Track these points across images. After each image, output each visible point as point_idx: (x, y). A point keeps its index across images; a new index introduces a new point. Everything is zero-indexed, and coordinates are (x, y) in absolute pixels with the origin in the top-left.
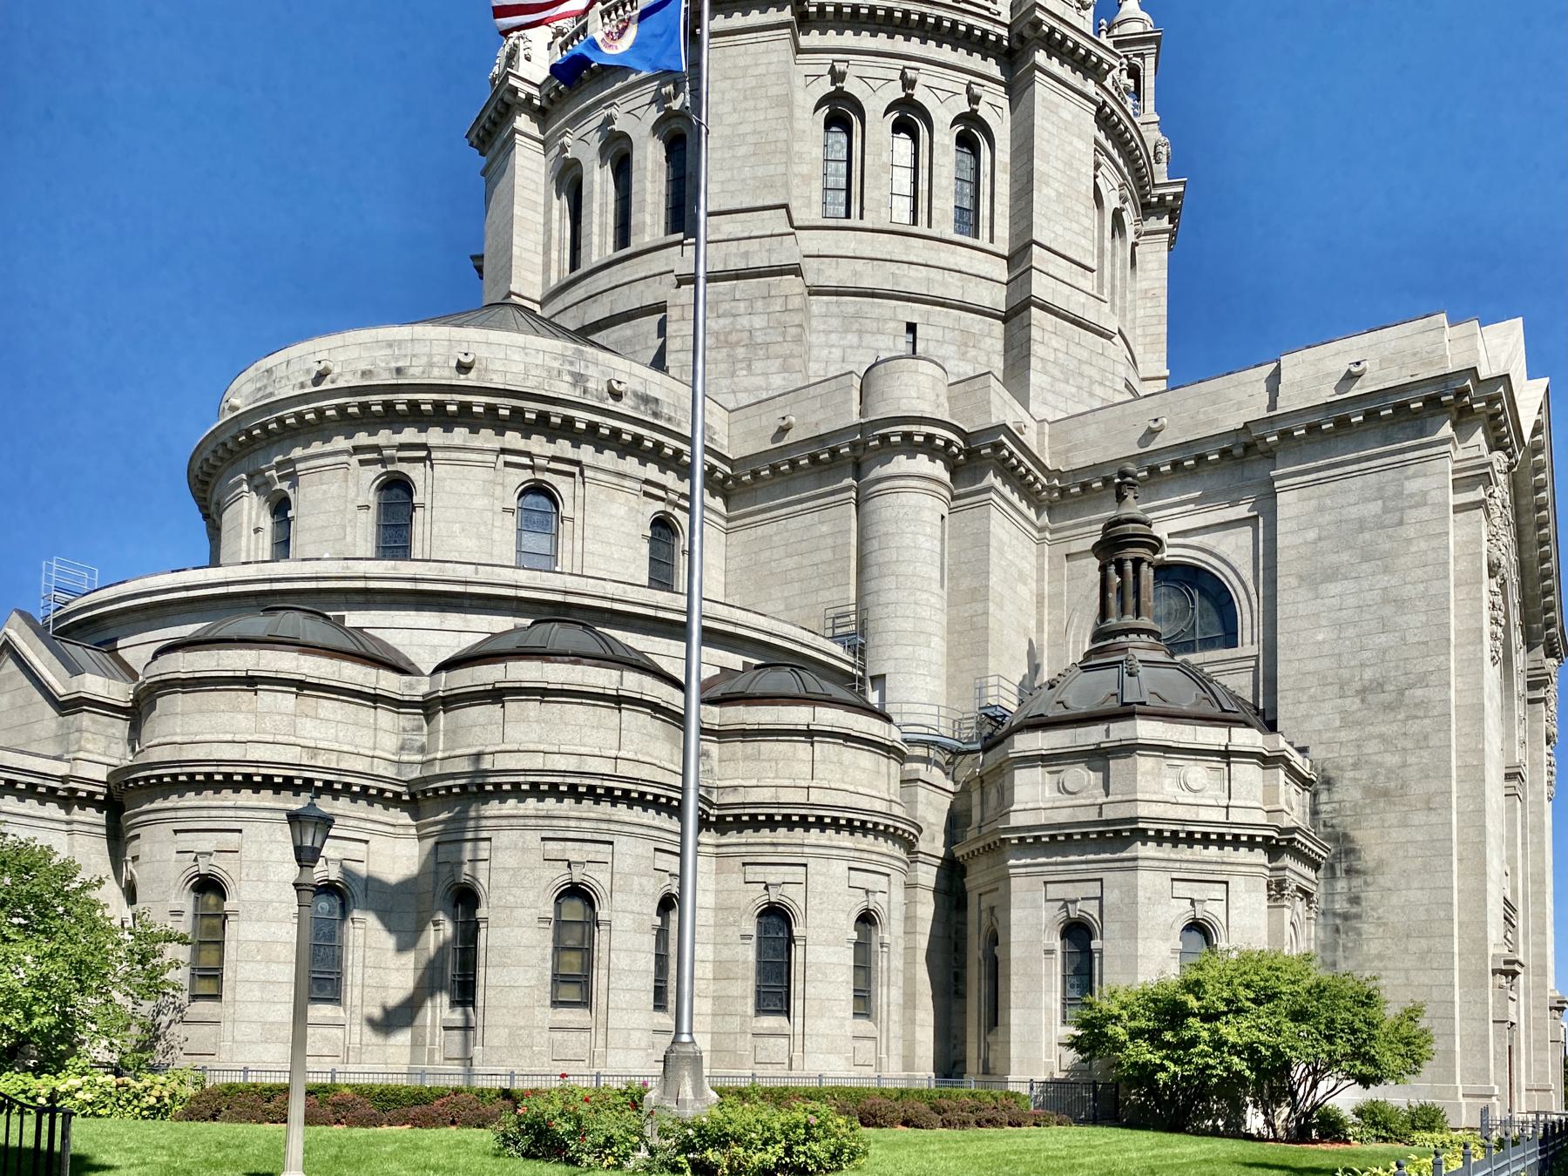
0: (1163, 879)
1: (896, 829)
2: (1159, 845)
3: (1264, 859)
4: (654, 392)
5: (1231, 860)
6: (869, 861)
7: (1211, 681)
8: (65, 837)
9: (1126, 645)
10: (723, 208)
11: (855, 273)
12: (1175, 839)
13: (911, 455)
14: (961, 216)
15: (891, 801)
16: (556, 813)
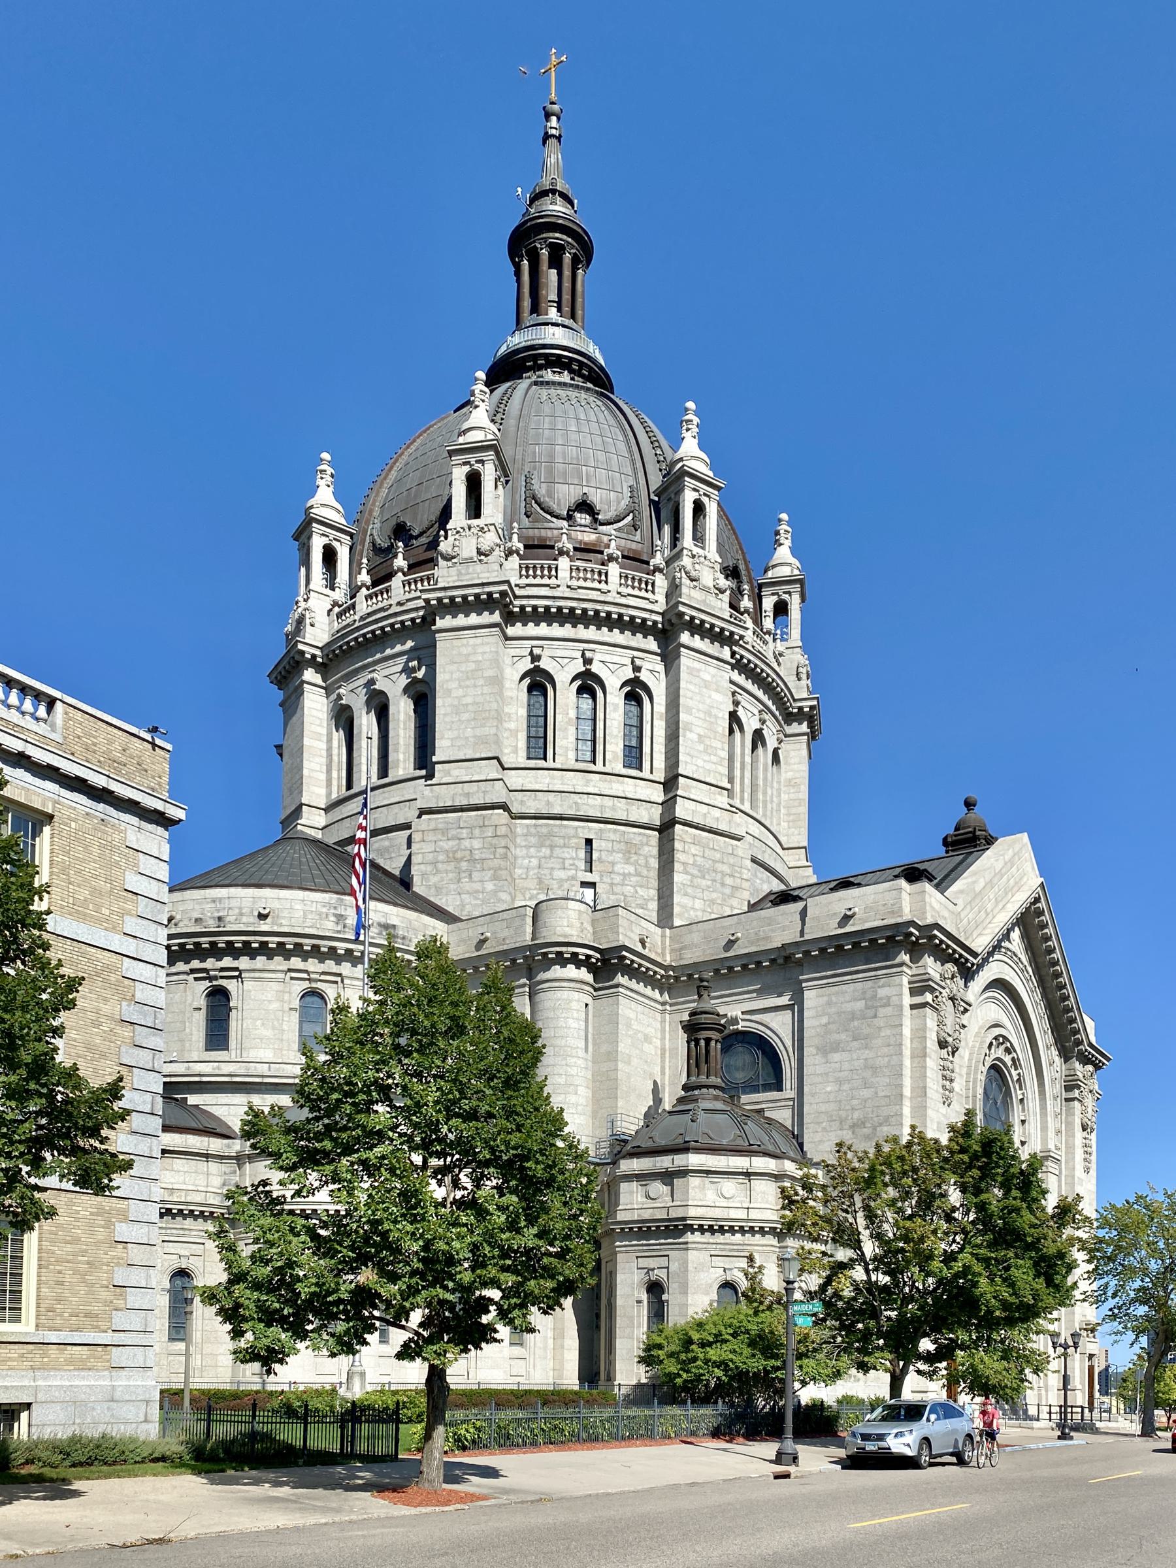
0: (704, 1256)
10: (452, 758)
11: (548, 803)
12: (711, 1229)
13: (563, 966)
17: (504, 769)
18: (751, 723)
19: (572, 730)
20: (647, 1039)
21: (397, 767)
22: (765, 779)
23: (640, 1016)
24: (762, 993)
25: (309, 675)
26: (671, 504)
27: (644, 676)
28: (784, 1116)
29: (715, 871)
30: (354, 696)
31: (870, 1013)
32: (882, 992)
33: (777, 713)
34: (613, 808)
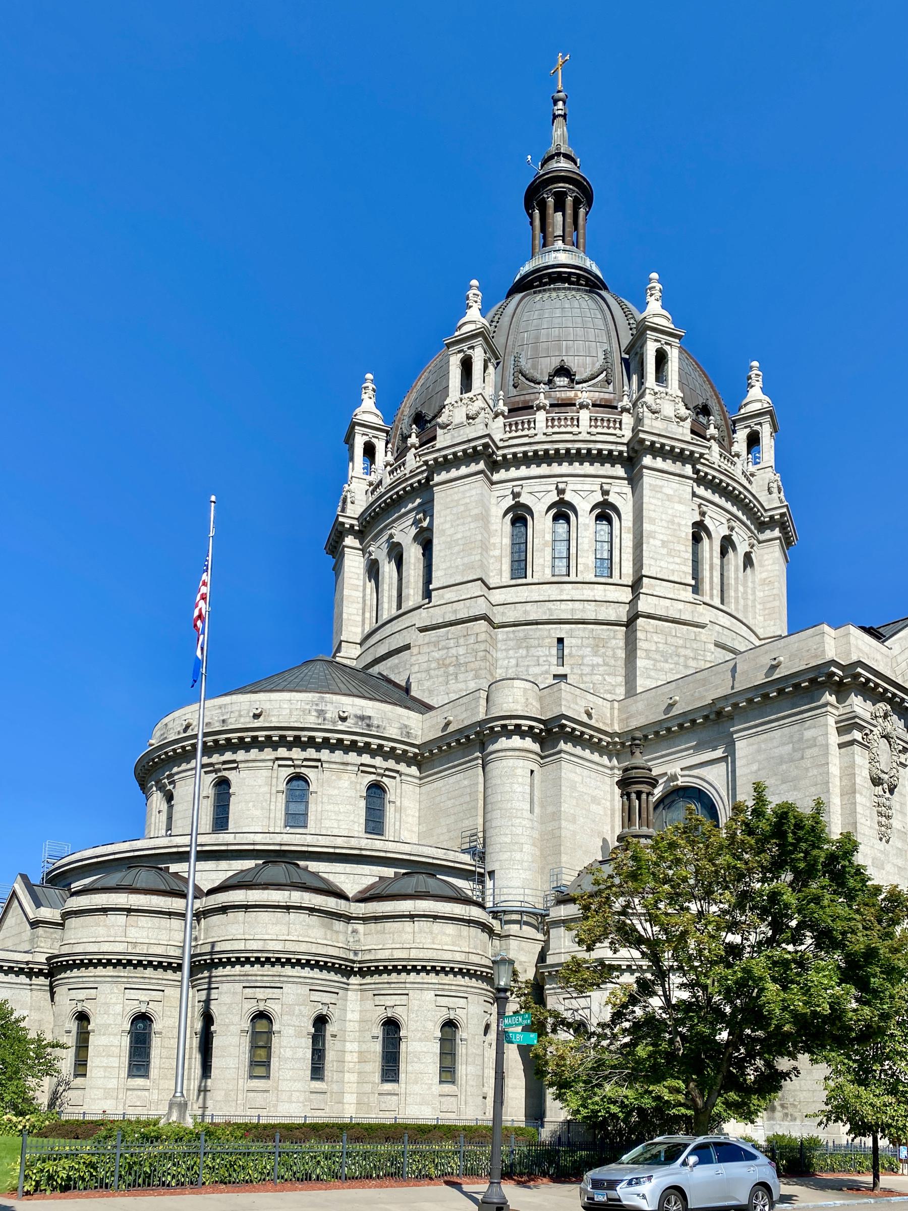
4: (366, 714)
8: (28, 992)
10: (445, 584)
11: (525, 612)
13: (509, 737)
17: (490, 589)
19: (549, 550)
20: (595, 800)
21: (408, 599)
22: (737, 579)
25: (349, 541)
26: (637, 358)
27: (612, 498)
29: (679, 656)
30: (379, 550)
31: (798, 755)
32: (808, 734)
33: (749, 523)
34: (583, 611)
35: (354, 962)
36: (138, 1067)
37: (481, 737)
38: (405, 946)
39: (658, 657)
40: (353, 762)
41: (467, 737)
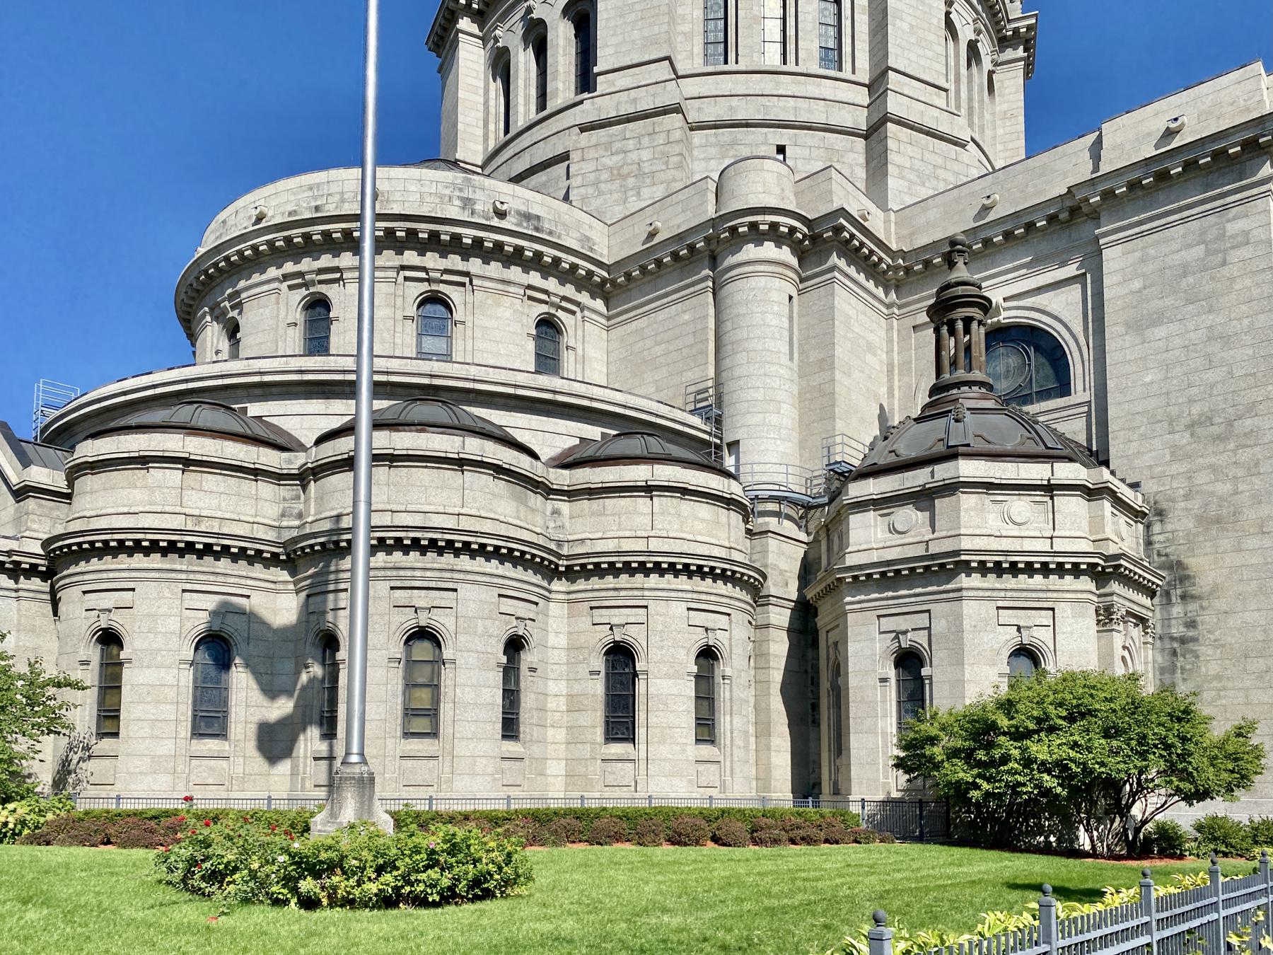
1: (734, 572)
2: (984, 575)
3: (1092, 586)
5: (1057, 588)
6: (708, 602)
7: (1037, 422)
8: (14, 603)
9: (958, 396)
10: (616, 66)
11: (731, 108)
12: (998, 569)
13: (759, 242)
14: (827, 55)
15: (730, 548)
16: (403, 565)
18: (966, 34)
21: (556, 96)
23: (861, 317)
24: (1038, 262)
25: (465, 23)
28: (1075, 429)
29: (937, 178)
30: (510, 34)
35: (559, 556)
36: (209, 720)
37: (713, 247)
38: (639, 534)
39: (913, 177)
40: (517, 280)
41: (691, 248)
